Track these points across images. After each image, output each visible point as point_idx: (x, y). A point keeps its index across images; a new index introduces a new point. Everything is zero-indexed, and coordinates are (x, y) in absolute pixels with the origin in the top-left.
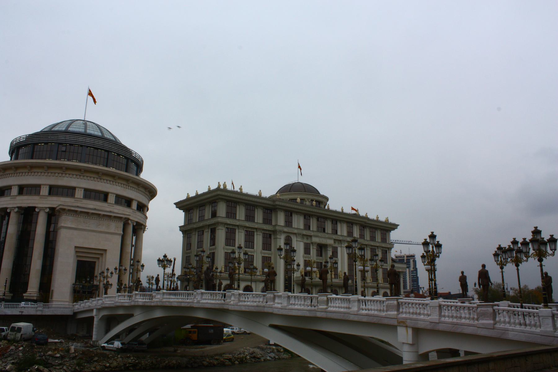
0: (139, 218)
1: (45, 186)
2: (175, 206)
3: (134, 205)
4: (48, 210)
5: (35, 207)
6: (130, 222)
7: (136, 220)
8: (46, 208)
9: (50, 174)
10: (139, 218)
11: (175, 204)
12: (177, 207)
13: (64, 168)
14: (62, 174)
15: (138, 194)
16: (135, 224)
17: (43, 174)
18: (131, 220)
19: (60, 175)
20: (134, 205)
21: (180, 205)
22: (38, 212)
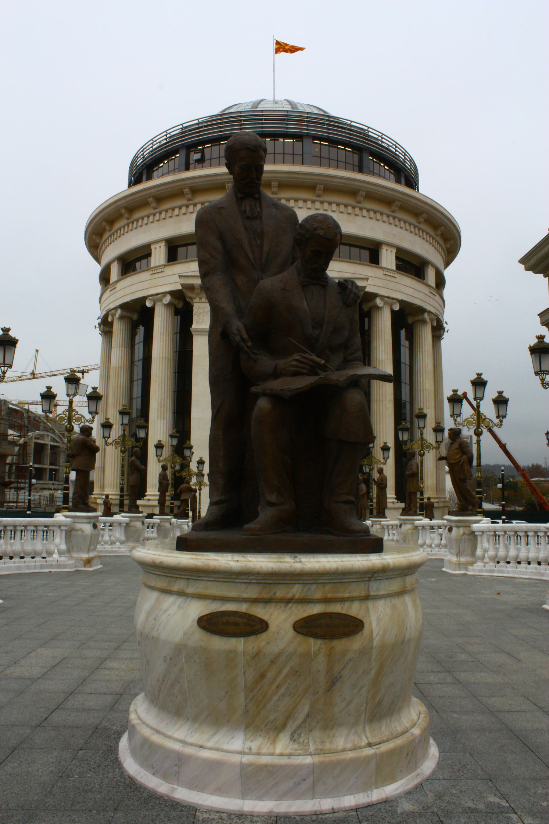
0: (411, 291)
1: (157, 246)
2: (522, 267)
3: (388, 258)
4: (168, 299)
5: (144, 299)
6: (378, 301)
7: (400, 297)
8: (164, 294)
9: (163, 215)
10: (411, 291)
11: (522, 261)
12: (527, 269)
13: (186, 190)
14: (187, 206)
15: (396, 231)
16: (397, 307)
17: (151, 219)
18: (382, 297)
19: (184, 210)
20: (388, 258)
21: (534, 260)
22: (152, 309)
